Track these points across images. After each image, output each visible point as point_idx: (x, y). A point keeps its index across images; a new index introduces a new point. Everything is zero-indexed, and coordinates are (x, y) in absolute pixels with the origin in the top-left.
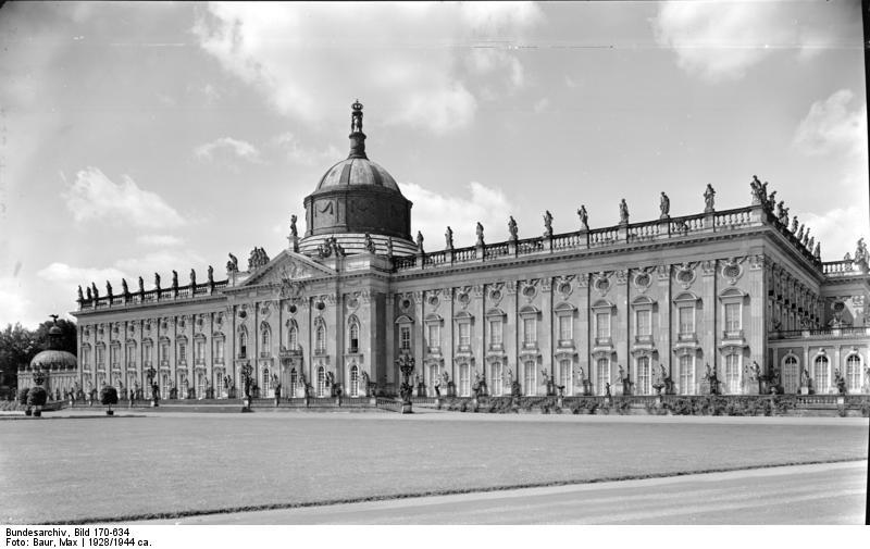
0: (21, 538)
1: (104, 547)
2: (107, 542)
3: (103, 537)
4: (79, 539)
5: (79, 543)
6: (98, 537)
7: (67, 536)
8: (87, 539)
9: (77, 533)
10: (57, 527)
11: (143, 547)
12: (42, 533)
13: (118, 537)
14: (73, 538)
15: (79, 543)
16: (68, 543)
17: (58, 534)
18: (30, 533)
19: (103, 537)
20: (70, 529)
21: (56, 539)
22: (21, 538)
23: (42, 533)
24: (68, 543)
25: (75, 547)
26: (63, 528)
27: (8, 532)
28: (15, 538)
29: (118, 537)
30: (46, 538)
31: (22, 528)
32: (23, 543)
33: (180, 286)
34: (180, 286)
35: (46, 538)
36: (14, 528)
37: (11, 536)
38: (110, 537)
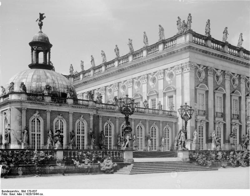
0: (6, 193)
1: (30, 195)
2: (31, 194)
3: (30, 192)
4: (23, 193)
6: (28, 193)
7: (19, 192)
8: (25, 193)
11: (41, 195)
12: (12, 192)
13: (34, 193)
14: (21, 193)
16: (20, 194)
17: (17, 192)
18: (9, 191)
19: (30, 192)
21: (16, 193)
22: (6, 193)
23: (12, 192)
24: (20, 194)
25: (21, 195)
27: (2, 191)
28: (4, 193)
29: (34, 193)
30: (13, 193)
31: (6, 190)
35: (13, 193)
36: (4, 190)
37: (3, 192)
38: (32, 192)
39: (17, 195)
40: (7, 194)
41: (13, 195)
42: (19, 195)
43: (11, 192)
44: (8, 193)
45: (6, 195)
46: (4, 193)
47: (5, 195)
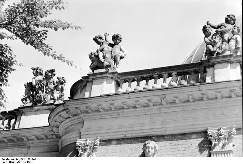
0: (6, 161)
4: (22, 161)
5: (22, 162)
7: (19, 160)
8: (24, 161)
9: (21, 159)
10: (16, 158)
12: (12, 160)
14: (20, 161)
15: (22, 162)
16: (19, 162)
17: (16, 160)
18: (8, 159)
20: (20, 158)
21: (16, 161)
22: (6, 161)
23: (12, 160)
24: (19, 162)
26: (18, 158)
27: (2, 159)
28: (4, 161)
30: (13, 161)
31: (6, 158)
32: (6, 162)
33: (49, 125)
34: (49, 125)
35: (13, 161)
36: (4, 158)
39: (16, 163)
40: (6, 162)
41: (12, 163)
42: (18, 163)
43: (11, 161)
44: (8, 161)
45: (6, 163)
46: (4, 161)
47: (5, 163)
